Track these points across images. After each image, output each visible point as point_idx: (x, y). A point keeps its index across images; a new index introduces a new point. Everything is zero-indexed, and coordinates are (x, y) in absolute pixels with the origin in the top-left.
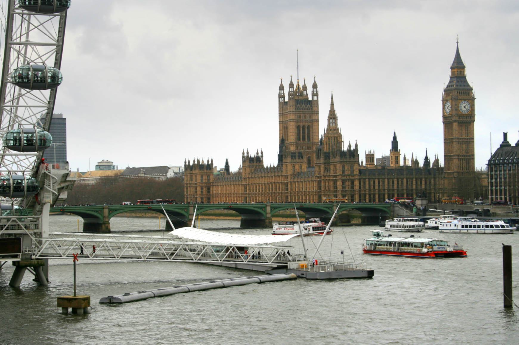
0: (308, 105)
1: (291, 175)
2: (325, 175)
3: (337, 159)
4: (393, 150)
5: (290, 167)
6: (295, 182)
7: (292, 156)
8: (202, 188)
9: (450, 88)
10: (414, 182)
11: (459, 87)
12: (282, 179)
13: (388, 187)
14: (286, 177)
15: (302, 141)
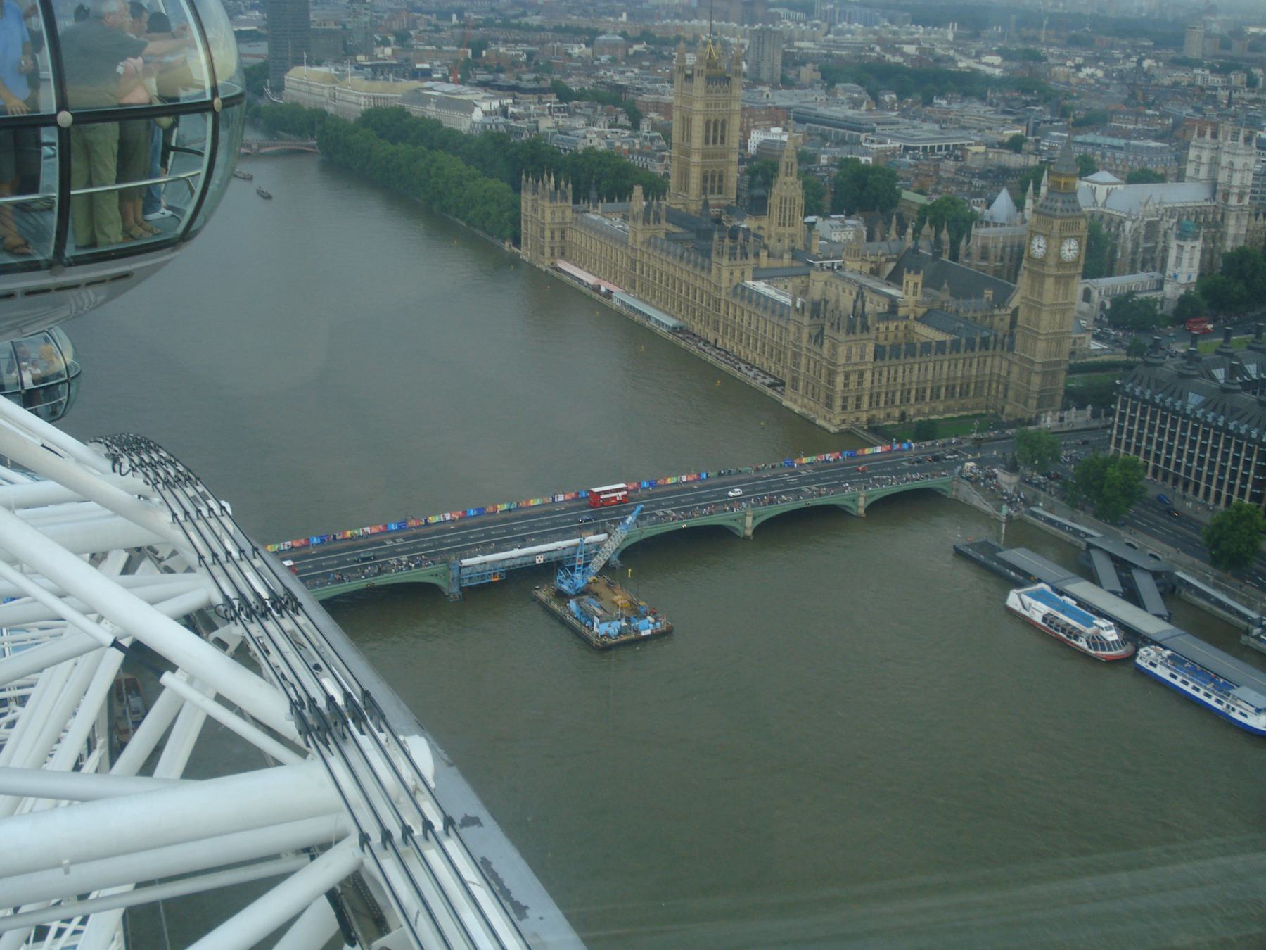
0: (726, 85)
1: (726, 288)
2: (809, 347)
3: (842, 336)
4: (912, 272)
5: (726, 274)
6: (735, 306)
7: (730, 254)
8: (553, 233)
9: (1047, 211)
10: (960, 366)
11: (1065, 214)
12: (706, 286)
13: (918, 378)
14: (718, 288)
15: (711, 146)
